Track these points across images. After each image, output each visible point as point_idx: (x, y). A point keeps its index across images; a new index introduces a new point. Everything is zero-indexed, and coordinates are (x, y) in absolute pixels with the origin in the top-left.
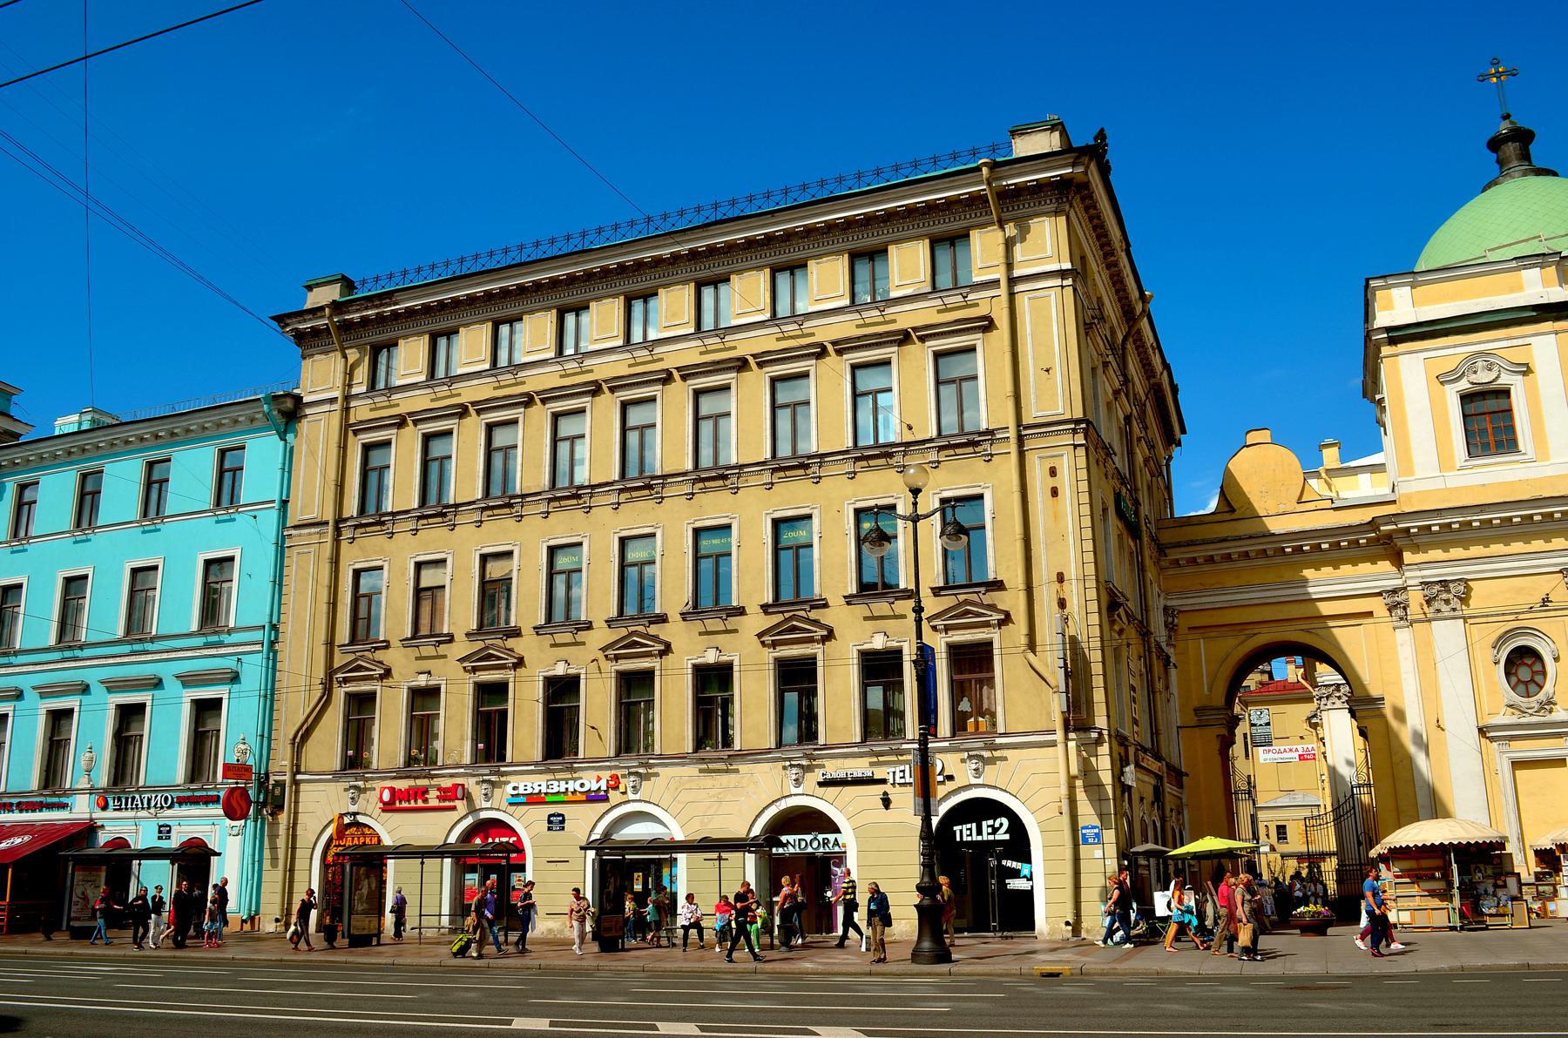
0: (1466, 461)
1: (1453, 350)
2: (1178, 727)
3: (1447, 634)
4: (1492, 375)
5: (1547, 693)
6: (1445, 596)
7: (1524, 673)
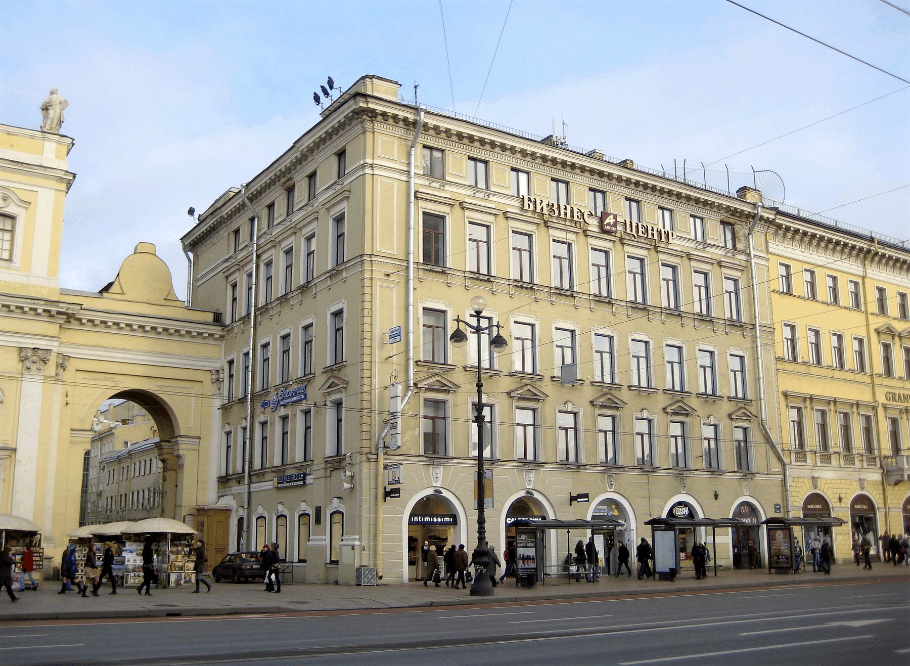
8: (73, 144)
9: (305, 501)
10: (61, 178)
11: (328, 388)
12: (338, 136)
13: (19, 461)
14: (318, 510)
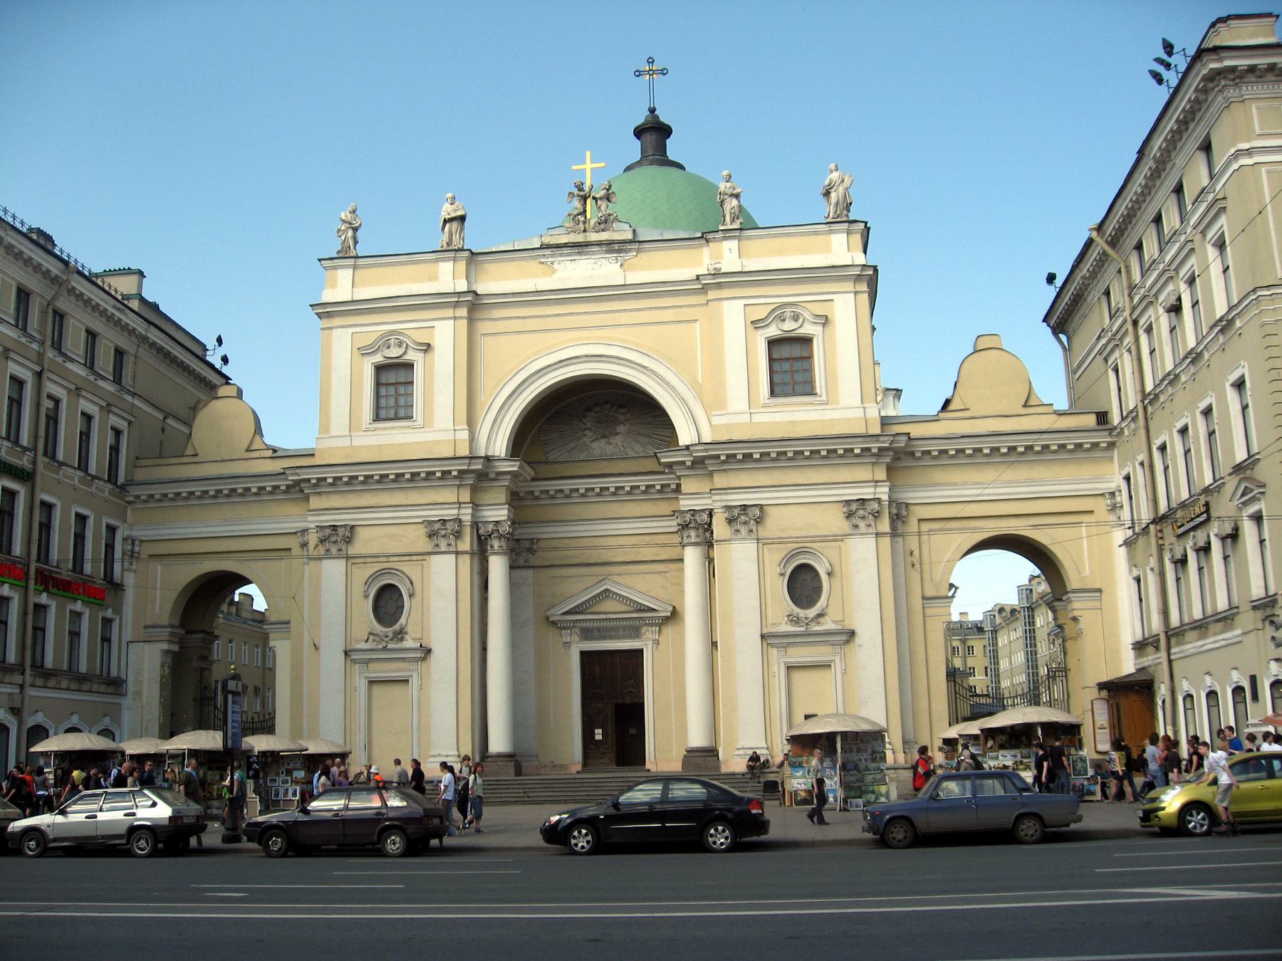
0: (370, 424)
1: (374, 328)
3: (333, 570)
4: (401, 351)
5: (401, 625)
6: (334, 539)
9: (1236, 669)
10: (859, 275)
11: (1243, 495)
12: (1196, 121)
13: (860, 646)
14: (1253, 680)
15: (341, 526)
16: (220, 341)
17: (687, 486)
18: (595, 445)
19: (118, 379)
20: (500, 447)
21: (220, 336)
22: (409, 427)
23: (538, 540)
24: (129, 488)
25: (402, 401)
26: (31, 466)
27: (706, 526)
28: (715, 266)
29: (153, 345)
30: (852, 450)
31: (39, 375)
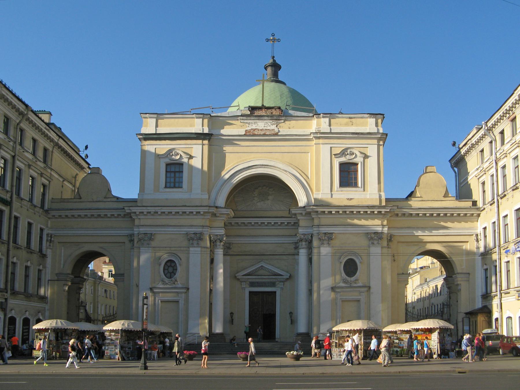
2: (48, 280)
7: (171, 270)
8: (384, 117)
15: (149, 233)
16: (86, 147)
17: (302, 223)
18: (259, 204)
19: (45, 162)
20: (221, 201)
21: (87, 145)
22: (181, 192)
23: (233, 243)
24: (50, 212)
25: (177, 180)
26: (10, 199)
27: (309, 241)
28: (318, 129)
29: (60, 147)
30: (374, 212)
31: (14, 157)
